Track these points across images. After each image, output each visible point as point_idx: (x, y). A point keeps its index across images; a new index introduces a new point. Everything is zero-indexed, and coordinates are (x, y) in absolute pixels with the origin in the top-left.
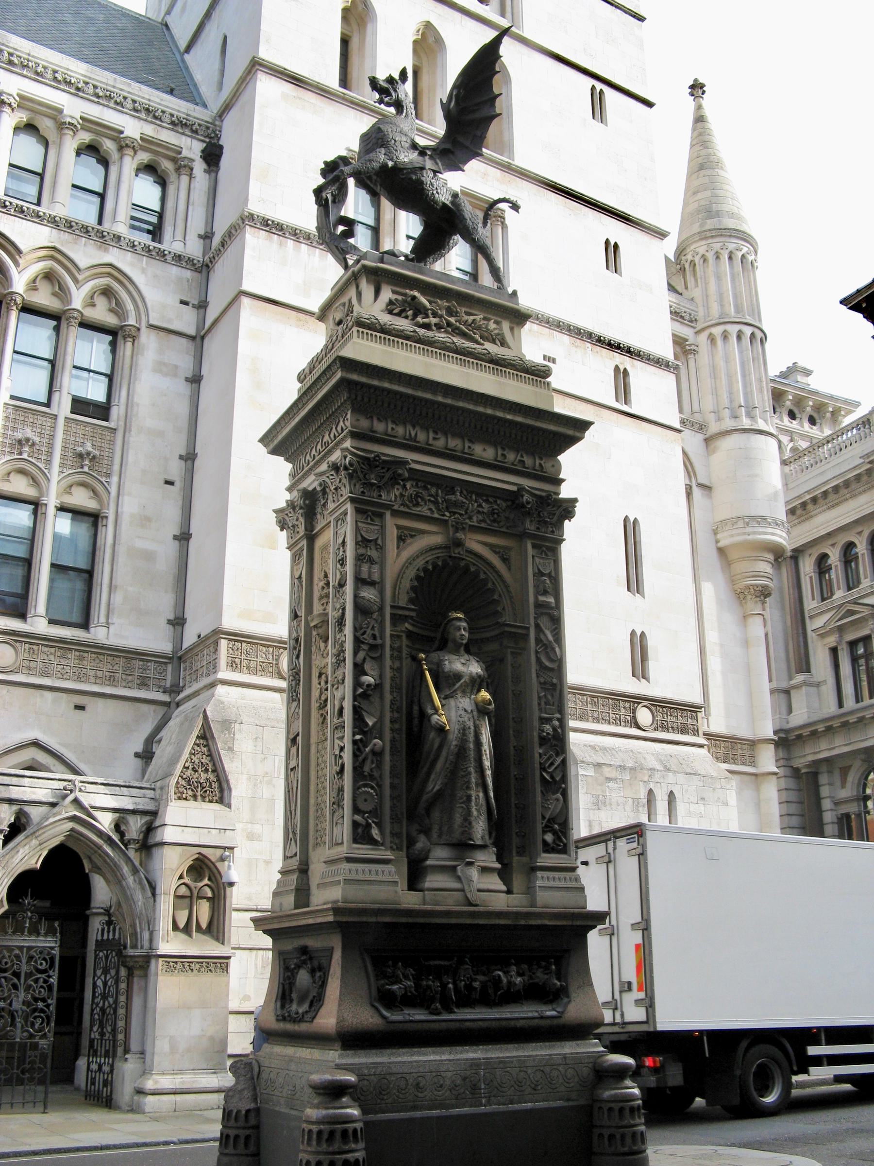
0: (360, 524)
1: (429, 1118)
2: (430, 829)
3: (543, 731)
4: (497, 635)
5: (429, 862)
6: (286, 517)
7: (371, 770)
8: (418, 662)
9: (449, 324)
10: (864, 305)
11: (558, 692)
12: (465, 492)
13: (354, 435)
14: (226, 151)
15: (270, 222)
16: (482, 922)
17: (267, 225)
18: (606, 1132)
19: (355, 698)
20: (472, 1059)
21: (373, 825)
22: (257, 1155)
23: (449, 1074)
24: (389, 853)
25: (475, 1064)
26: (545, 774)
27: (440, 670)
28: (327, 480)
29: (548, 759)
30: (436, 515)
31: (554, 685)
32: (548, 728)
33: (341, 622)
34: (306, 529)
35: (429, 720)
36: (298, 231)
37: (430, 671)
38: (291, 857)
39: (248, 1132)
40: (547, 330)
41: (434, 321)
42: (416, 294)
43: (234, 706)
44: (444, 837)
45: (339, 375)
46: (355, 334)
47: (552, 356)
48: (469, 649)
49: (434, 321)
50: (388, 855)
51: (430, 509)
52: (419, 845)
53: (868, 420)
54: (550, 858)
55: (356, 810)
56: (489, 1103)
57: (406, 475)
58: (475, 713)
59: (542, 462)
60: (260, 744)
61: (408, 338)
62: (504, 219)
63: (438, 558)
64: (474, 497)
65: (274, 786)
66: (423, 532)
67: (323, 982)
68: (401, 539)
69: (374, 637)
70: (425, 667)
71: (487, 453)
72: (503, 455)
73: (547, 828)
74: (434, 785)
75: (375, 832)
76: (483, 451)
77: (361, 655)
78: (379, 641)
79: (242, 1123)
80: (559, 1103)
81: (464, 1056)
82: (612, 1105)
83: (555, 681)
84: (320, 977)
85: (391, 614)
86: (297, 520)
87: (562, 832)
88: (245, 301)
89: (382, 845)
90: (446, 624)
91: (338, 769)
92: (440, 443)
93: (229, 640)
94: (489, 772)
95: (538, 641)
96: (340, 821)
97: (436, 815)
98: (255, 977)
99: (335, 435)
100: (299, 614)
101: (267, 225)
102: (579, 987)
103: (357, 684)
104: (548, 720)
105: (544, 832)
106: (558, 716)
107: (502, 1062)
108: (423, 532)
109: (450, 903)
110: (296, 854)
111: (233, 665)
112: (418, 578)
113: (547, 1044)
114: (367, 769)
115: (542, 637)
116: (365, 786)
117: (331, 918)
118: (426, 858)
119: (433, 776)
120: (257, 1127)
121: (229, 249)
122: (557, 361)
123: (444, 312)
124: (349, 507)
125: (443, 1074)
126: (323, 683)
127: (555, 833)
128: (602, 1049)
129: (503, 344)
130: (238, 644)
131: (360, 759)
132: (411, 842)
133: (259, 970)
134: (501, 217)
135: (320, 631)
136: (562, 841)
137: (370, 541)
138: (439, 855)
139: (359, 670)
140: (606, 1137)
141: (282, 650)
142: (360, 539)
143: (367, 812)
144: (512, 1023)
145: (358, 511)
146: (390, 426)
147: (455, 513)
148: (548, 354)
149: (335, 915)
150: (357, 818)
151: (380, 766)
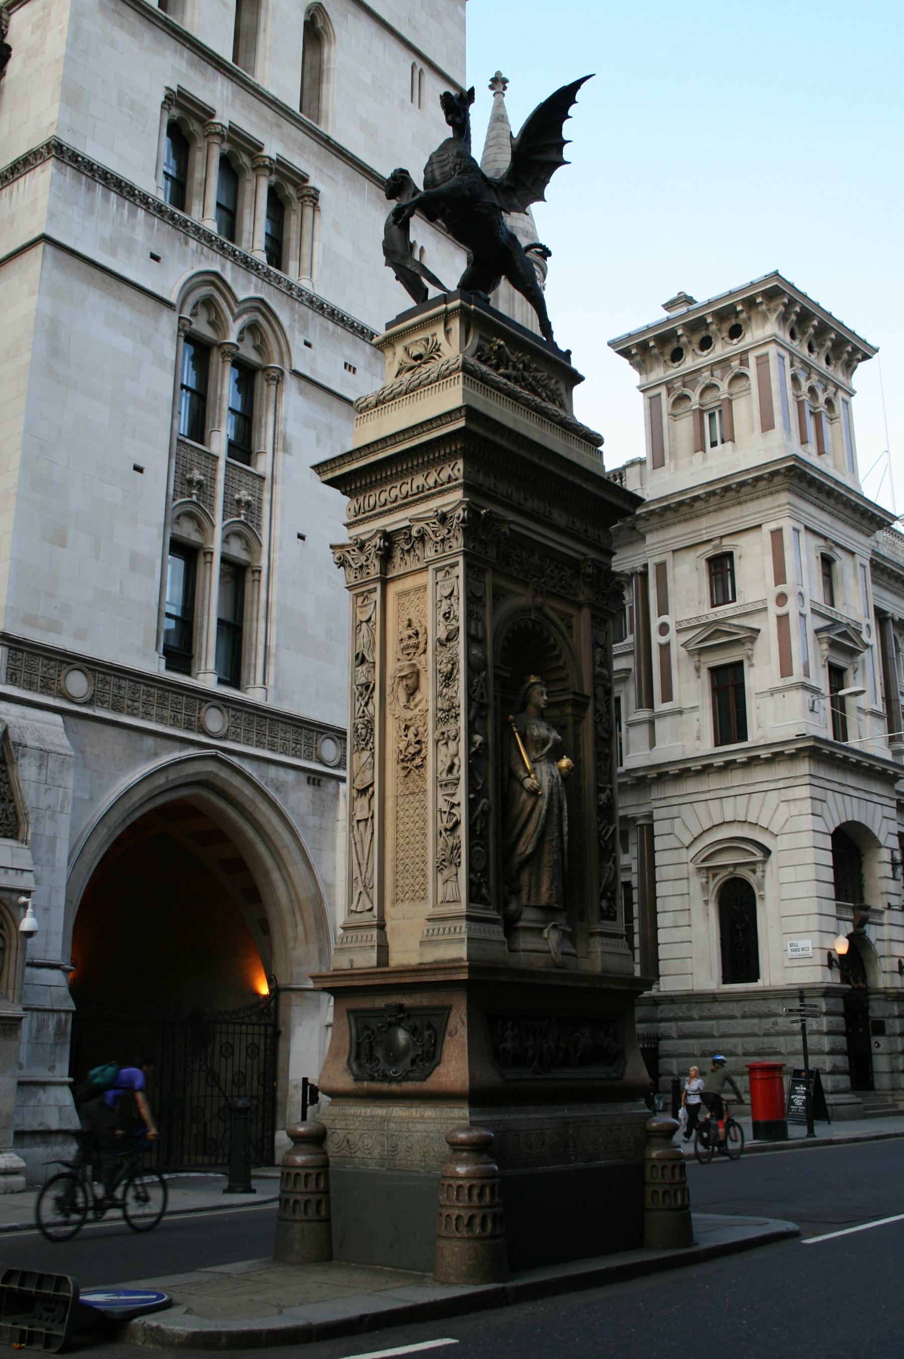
0: (469, 579)
2: (520, 891)
3: (600, 800)
4: (563, 701)
5: (521, 924)
6: (347, 554)
7: (482, 829)
8: (508, 724)
9: (524, 379)
10: (634, 351)
13: (468, 488)
14: (13, 53)
15: (80, 159)
16: (570, 984)
17: (77, 161)
18: (660, 1190)
19: (470, 756)
22: (328, 1220)
24: (495, 913)
26: (602, 842)
27: (528, 732)
28: (426, 527)
29: (604, 828)
30: (521, 577)
31: (607, 755)
32: (603, 797)
33: (449, 678)
34: (381, 572)
35: (522, 785)
36: (109, 176)
37: (519, 734)
38: (361, 912)
39: (319, 1197)
40: (350, 335)
41: (514, 373)
42: (502, 343)
43: (15, 726)
44: (533, 899)
45: (461, 424)
46: (461, 379)
47: (353, 365)
48: (542, 715)
49: (514, 373)
50: (493, 914)
51: (516, 570)
52: (513, 907)
53: (621, 474)
55: (471, 869)
57: (508, 532)
58: (560, 779)
60: (44, 772)
61: (500, 390)
62: (317, 200)
63: (522, 620)
64: (548, 560)
65: (56, 822)
67: (436, 1040)
68: (496, 597)
69: (482, 696)
70: (515, 729)
71: (560, 518)
72: (573, 522)
74: (526, 846)
77: (473, 712)
78: (485, 700)
79: (311, 1186)
82: (666, 1163)
84: (430, 1035)
85: (494, 674)
86: (367, 560)
88: (49, 249)
90: (529, 687)
91: (451, 825)
93: (10, 648)
94: (566, 838)
95: (596, 711)
96: (454, 878)
97: (525, 877)
98: (29, 1042)
99: (436, 481)
100: (370, 659)
101: (77, 161)
103: (470, 743)
105: (601, 899)
109: (539, 963)
110: (371, 910)
111: (12, 678)
114: (478, 827)
115: (599, 706)
116: (477, 845)
117: (465, 976)
118: (519, 919)
119: (523, 840)
120: (327, 1192)
121: (22, 180)
122: (357, 371)
123: (521, 366)
124: (461, 559)
126: (411, 735)
127: (608, 900)
128: (648, 1111)
129: (562, 406)
130: (19, 654)
131: (474, 817)
132: (506, 903)
133: (34, 1034)
134: (314, 198)
135: (410, 682)
137: (477, 597)
138: (529, 917)
139: (471, 729)
140: (661, 1193)
141: (64, 665)
142: (470, 595)
143: (479, 872)
145: (468, 567)
146: (492, 481)
147: (534, 576)
148: (349, 363)
149: (470, 973)
150: (472, 876)
151: (487, 826)
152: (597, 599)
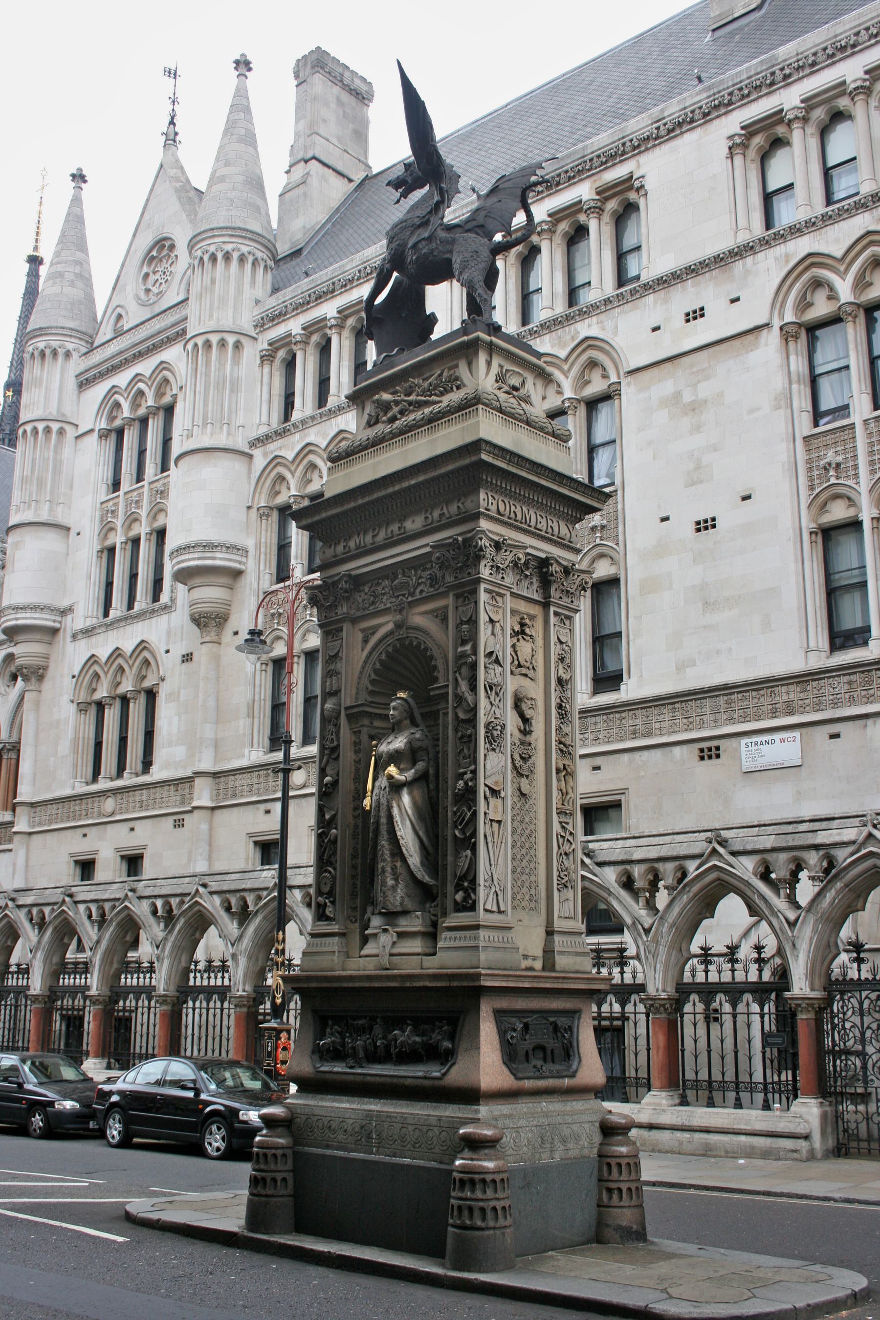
1: (335, 1157)
9: (410, 403)
11: (473, 742)
12: (406, 570)
16: (377, 985)
20: (369, 1111)
21: (329, 904)
23: (351, 1121)
25: (369, 1114)
26: (457, 833)
41: (396, 409)
54: (457, 917)
56: (378, 1153)
58: (387, 789)
59: (460, 505)
64: (413, 572)
66: (380, 626)
73: (458, 887)
75: (329, 911)
76: (414, 524)
80: (434, 1164)
81: (367, 1107)
83: (469, 732)
87: (472, 888)
89: (334, 920)
92: (382, 536)
102: (466, 1050)
104: (461, 776)
105: (457, 892)
106: (472, 767)
107: (389, 1116)
108: (380, 626)
112: (432, 657)
113: (434, 1104)
116: (326, 871)
125: (347, 1121)
127: (466, 890)
136: (471, 899)
144: (401, 1081)
147: (398, 596)
151: (335, 853)
152: (456, 577)
